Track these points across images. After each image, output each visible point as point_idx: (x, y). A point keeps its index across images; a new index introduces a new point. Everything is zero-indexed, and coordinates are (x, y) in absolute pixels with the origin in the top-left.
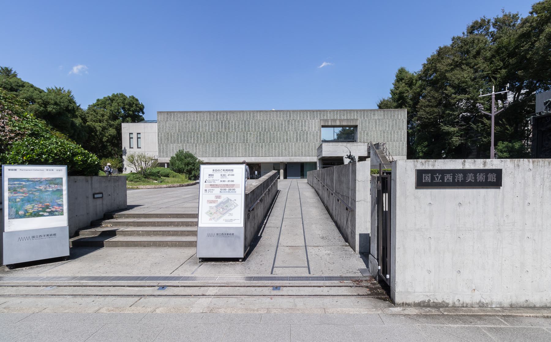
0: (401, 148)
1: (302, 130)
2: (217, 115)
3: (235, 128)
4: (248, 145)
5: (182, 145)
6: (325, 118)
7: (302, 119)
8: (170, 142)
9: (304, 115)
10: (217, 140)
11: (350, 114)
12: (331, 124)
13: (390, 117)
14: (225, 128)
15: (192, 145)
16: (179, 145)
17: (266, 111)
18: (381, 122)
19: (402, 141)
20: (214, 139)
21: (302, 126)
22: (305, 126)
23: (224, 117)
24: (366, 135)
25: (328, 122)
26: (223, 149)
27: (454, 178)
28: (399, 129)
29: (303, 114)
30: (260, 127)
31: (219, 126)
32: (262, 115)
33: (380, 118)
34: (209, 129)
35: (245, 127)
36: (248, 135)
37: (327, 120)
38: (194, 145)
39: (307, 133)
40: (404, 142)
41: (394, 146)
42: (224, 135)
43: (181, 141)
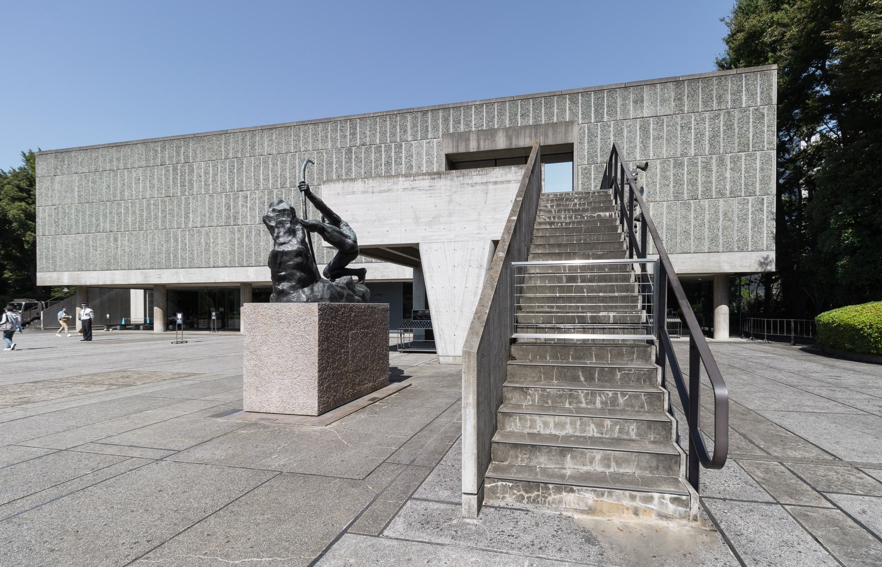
0: (750, 220)
2: (163, 148)
3: (205, 185)
5: (86, 238)
6: (462, 128)
9: (395, 127)
11: (549, 107)
12: (479, 146)
13: (705, 103)
14: (183, 186)
16: (81, 237)
17: (287, 127)
18: (668, 126)
21: (388, 163)
23: (179, 155)
25: (468, 140)
28: (744, 147)
29: (391, 124)
30: (268, 175)
32: (274, 138)
33: (661, 111)
37: (464, 137)
38: (112, 236)
40: (765, 197)
41: (721, 215)
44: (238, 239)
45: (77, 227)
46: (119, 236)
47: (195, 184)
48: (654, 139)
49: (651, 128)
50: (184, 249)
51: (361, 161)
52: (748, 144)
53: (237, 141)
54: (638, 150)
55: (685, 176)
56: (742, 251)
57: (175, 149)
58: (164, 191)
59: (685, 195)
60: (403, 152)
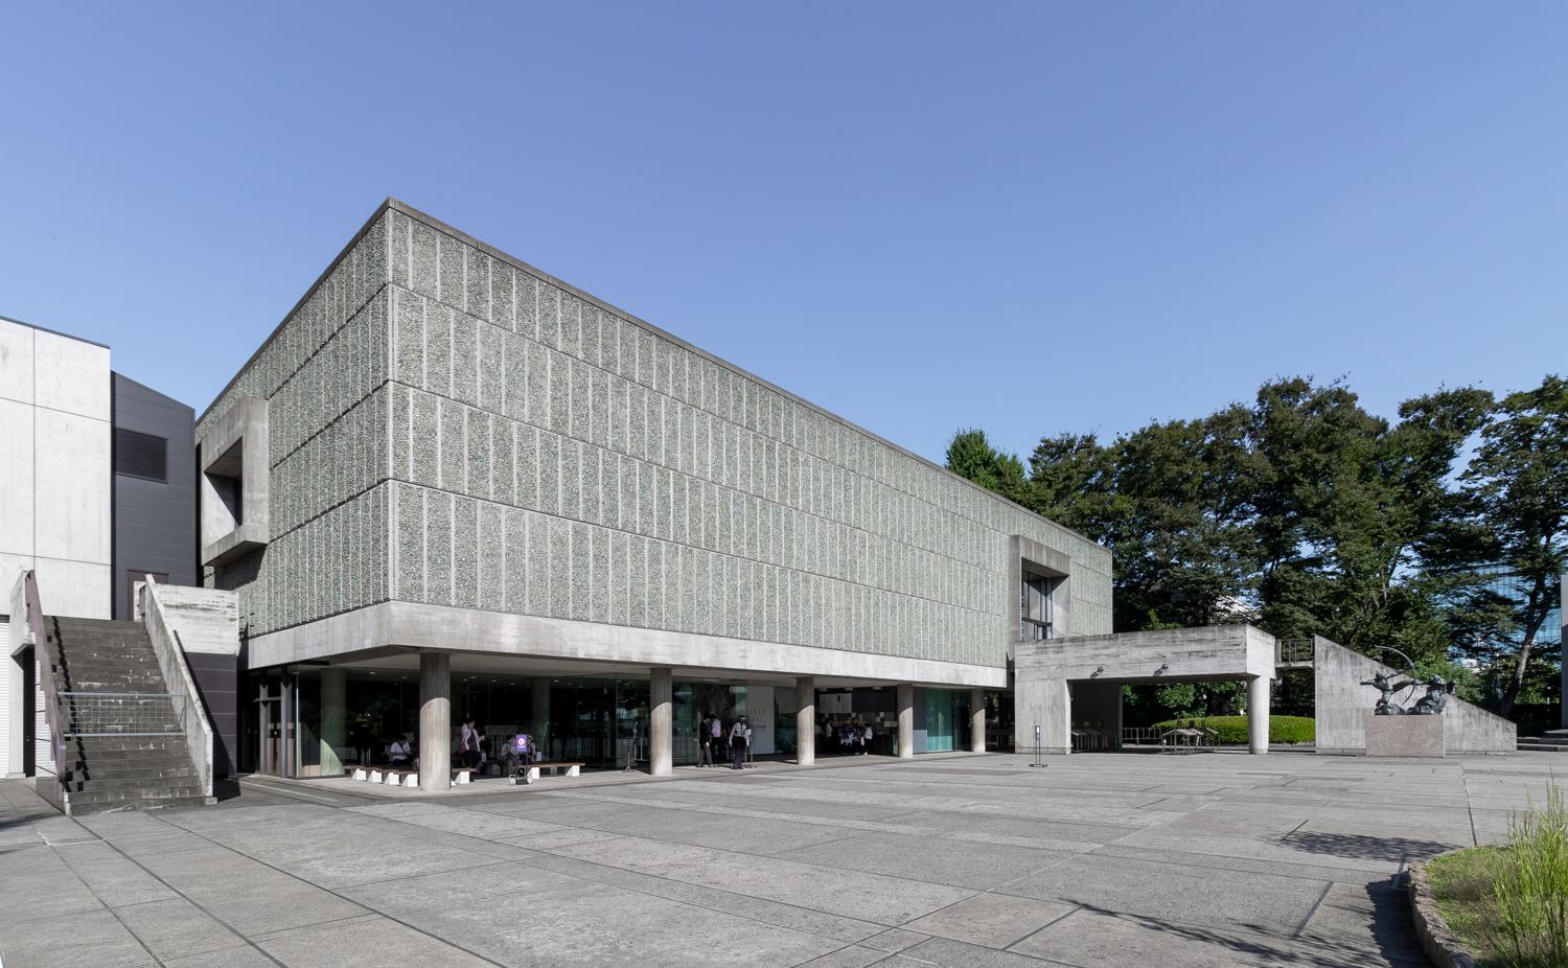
5: (576, 532)
8: (492, 487)
43: (568, 503)
45: (549, 496)
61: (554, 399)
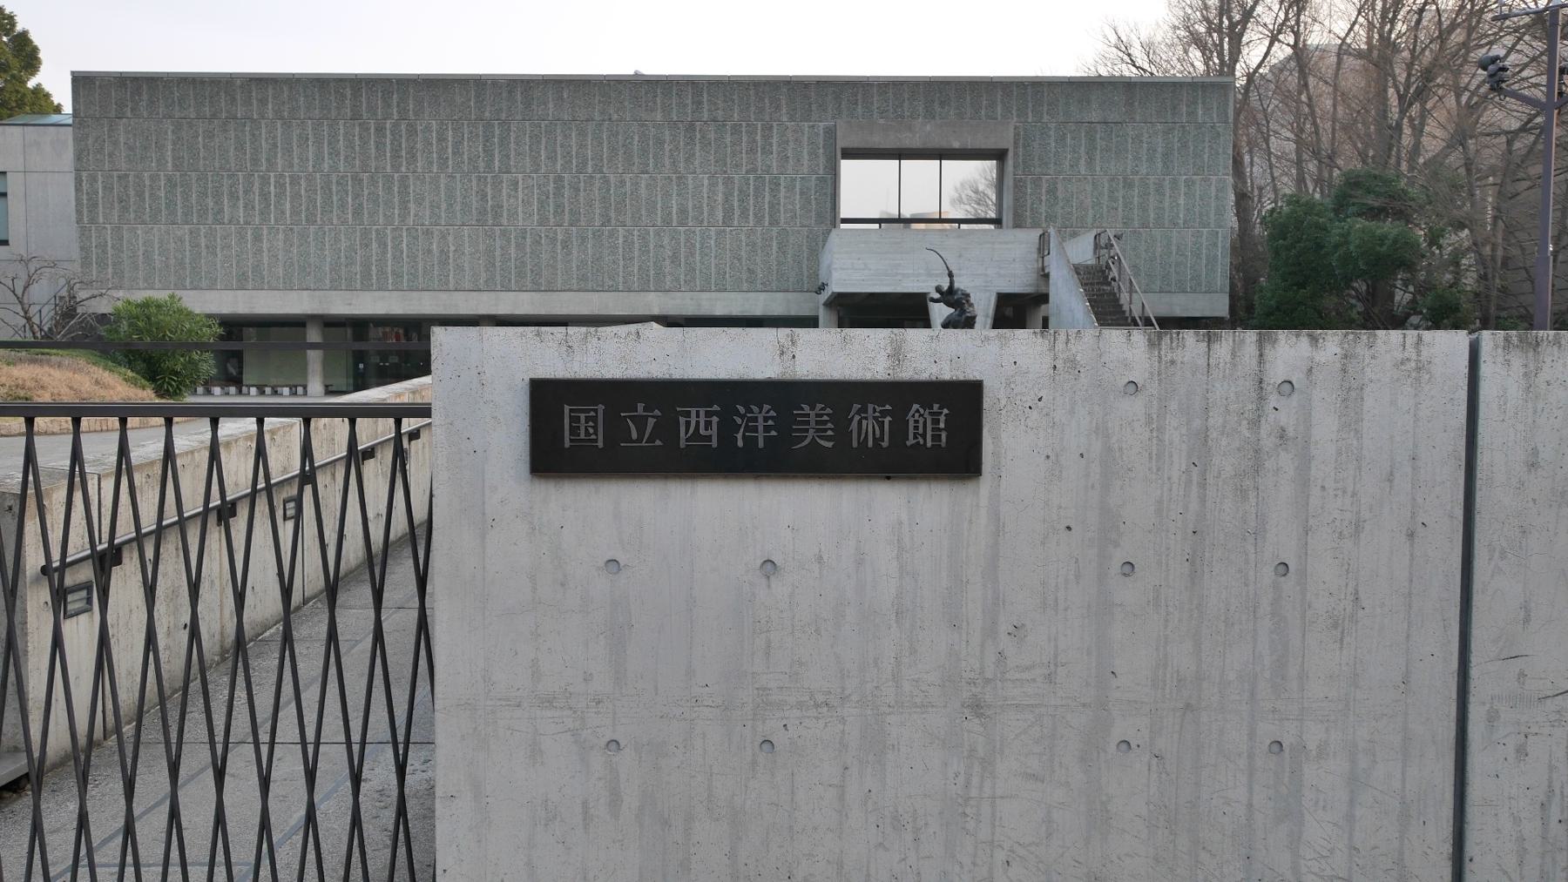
1: (754, 170)
3: (440, 158)
4: (504, 234)
7: (753, 117)
9: (762, 99)
10: (357, 212)
14: (396, 155)
15: (242, 238)
19: (1207, 225)
20: (343, 206)
21: (752, 151)
22: (767, 151)
23: (389, 106)
24: (1044, 198)
26: (384, 253)
27: (727, 429)
30: (556, 152)
31: (364, 143)
34: (319, 158)
35: (488, 152)
36: (500, 191)
39: (776, 184)
40: (1220, 230)
41: (1174, 248)
42: (389, 190)
44: (502, 248)
46: (265, 232)
47: (419, 154)
48: (1101, 150)
49: (1098, 136)
50: (397, 258)
51: (710, 144)
52: (1203, 167)
53: (500, 94)
54: (1082, 162)
55: (1136, 199)
56: (1195, 292)
57: (380, 94)
58: (357, 162)
59: (1136, 223)
60: (775, 137)
61: (173, 150)
